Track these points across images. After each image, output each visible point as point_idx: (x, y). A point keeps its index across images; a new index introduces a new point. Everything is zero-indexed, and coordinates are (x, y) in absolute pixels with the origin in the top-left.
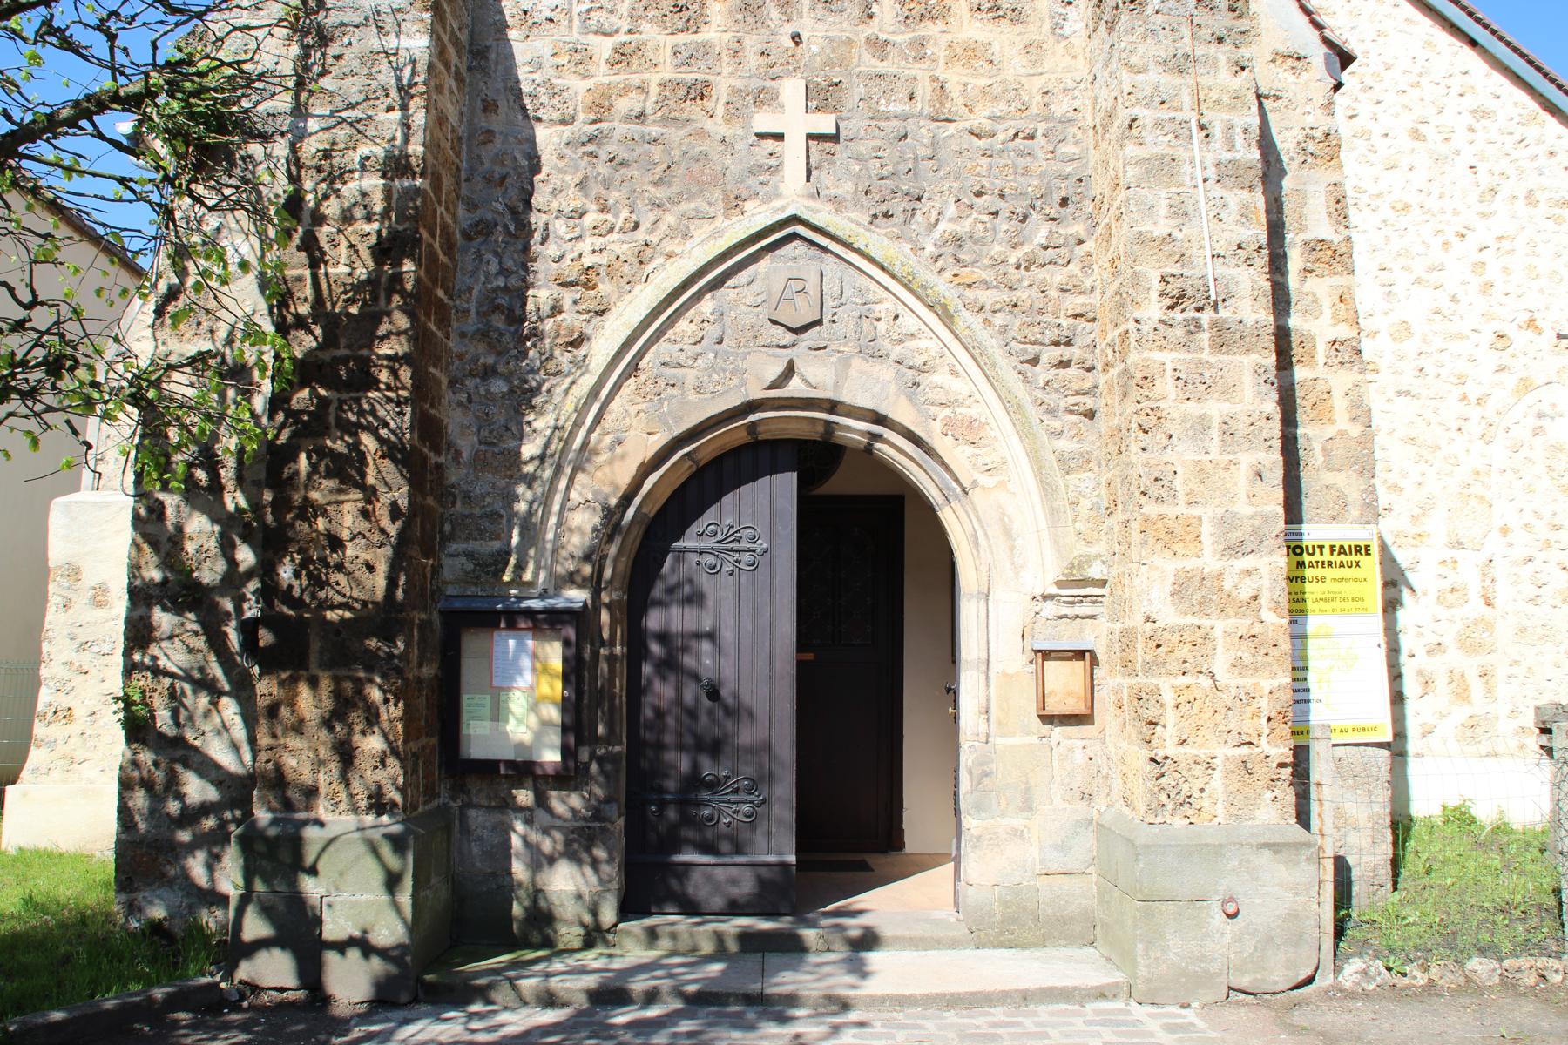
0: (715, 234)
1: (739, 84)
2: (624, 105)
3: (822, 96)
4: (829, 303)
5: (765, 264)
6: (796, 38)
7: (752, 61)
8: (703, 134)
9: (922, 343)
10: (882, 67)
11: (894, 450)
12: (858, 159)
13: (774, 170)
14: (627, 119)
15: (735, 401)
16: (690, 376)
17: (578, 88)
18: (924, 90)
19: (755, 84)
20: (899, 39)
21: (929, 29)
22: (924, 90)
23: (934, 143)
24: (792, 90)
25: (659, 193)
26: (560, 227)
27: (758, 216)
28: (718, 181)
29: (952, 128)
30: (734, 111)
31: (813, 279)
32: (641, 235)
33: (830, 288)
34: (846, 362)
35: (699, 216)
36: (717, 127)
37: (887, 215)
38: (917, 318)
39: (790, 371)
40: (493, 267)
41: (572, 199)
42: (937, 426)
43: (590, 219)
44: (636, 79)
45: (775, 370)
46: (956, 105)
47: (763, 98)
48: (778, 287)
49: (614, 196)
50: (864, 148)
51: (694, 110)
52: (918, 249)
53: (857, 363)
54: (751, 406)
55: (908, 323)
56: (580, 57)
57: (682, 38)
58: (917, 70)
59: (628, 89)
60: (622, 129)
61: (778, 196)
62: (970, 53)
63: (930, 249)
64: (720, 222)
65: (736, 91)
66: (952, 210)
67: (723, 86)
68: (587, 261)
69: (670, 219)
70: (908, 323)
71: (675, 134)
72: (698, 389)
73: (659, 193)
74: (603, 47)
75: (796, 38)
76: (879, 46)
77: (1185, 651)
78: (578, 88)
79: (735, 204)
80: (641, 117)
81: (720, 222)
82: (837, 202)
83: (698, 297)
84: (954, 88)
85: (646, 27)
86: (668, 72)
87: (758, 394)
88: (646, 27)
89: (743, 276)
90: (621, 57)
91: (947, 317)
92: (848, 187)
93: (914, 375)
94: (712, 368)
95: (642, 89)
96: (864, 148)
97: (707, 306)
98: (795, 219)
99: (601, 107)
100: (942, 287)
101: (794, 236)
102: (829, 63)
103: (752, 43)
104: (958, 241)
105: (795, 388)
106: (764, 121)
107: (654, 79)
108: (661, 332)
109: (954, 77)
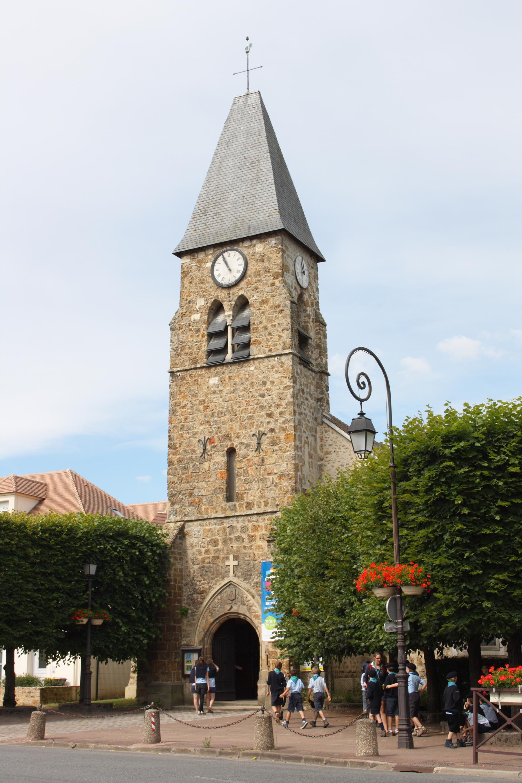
0: (220, 584)
1: (223, 556)
2: (207, 561)
3: (236, 558)
4: (237, 595)
5: (227, 589)
6: (232, 547)
7: (225, 552)
8: (218, 565)
9: (250, 602)
10: (245, 551)
11: (248, 620)
12: (242, 569)
13: (229, 572)
14: (207, 563)
15: (223, 613)
16: (217, 609)
17: (200, 558)
18: (252, 555)
19: (226, 556)
20: (248, 545)
21: (253, 543)
22: (252, 555)
23: (254, 565)
24: (231, 557)
25: (212, 576)
26: (198, 583)
27: (226, 581)
28: (221, 573)
29: (256, 562)
30: (223, 562)
31: (234, 591)
32: (210, 584)
33: (237, 592)
34: (239, 606)
35: (218, 581)
36: (220, 564)
37: (246, 579)
38: (250, 597)
39: (231, 607)
40: (188, 591)
41: (200, 578)
42: (253, 616)
43: (202, 582)
44: (208, 556)
45: (229, 607)
46: (257, 557)
47: (227, 558)
48: (229, 593)
49: (206, 577)
50: (243, 566)
51: (217, 561)
52: (250, 585)
53: (241, 606)
54: (226, 614)
55: (249, 598)
56: (200, 552)
57: (215, 548)
58: (251, 551)
59: (207, 558)
60: (207, 565)
61: (229, 576)
62: (259, 547)
63: (252, 585)
64: (221, 582)
65: (223, 558)
66: (256, 577)
67: (222, 556)
68: (202, 589)
69: (214, 581)
70: (249, 598)
71: (215, 566)
72: (218, 611)
73: (212, 576)
74: (203, 550)
75: (232, 547)
76: (245, 547)
77: (273, 655)
78: (200, 558)
79: (223, 579)
80: (209, 563)
81: (221, 582)
82: (238, 577)
83: (217, 595)
84: (256, 555)
85: (210, 546)
86: (213, 555)
87: (227, 612)
88: (210, 546)
89: (224, 591)
90: (207, 552)
91: (253, 597)
92: (240, 574)
93: (249, 609)
94: (220, 608)
95: (209, 558)
96: (243, 566)
97: (219, 597)
98: (231, 581)
99: (203, 561)
100: (254, 591)
101: (231, 584)
102: (237, 551)
103: (225, 548)
104: (257, 583)
105: (232, 610)
106: (227, 563)
107: (211, 556)
108: (212, 601)
109: (256, 552)
